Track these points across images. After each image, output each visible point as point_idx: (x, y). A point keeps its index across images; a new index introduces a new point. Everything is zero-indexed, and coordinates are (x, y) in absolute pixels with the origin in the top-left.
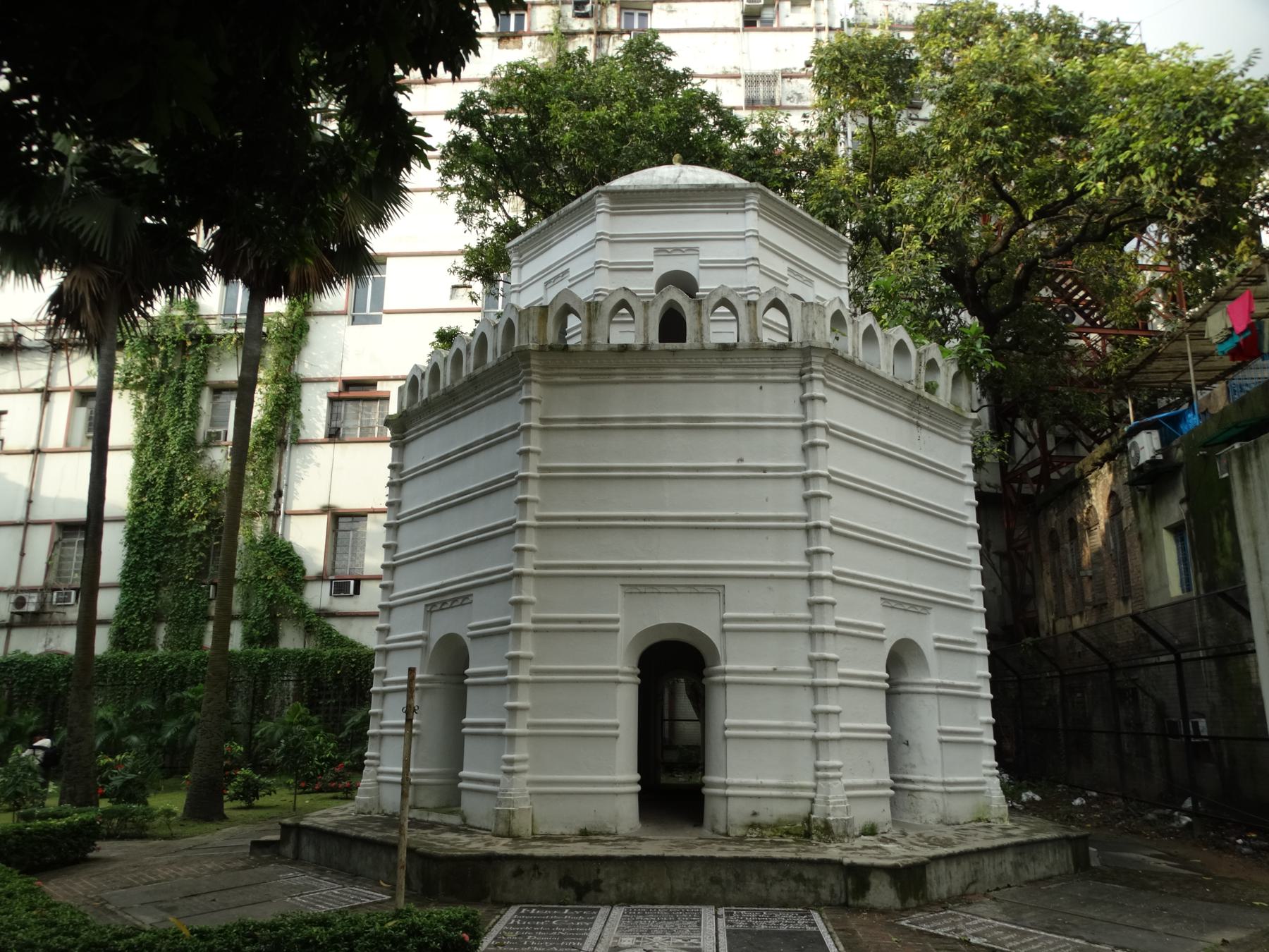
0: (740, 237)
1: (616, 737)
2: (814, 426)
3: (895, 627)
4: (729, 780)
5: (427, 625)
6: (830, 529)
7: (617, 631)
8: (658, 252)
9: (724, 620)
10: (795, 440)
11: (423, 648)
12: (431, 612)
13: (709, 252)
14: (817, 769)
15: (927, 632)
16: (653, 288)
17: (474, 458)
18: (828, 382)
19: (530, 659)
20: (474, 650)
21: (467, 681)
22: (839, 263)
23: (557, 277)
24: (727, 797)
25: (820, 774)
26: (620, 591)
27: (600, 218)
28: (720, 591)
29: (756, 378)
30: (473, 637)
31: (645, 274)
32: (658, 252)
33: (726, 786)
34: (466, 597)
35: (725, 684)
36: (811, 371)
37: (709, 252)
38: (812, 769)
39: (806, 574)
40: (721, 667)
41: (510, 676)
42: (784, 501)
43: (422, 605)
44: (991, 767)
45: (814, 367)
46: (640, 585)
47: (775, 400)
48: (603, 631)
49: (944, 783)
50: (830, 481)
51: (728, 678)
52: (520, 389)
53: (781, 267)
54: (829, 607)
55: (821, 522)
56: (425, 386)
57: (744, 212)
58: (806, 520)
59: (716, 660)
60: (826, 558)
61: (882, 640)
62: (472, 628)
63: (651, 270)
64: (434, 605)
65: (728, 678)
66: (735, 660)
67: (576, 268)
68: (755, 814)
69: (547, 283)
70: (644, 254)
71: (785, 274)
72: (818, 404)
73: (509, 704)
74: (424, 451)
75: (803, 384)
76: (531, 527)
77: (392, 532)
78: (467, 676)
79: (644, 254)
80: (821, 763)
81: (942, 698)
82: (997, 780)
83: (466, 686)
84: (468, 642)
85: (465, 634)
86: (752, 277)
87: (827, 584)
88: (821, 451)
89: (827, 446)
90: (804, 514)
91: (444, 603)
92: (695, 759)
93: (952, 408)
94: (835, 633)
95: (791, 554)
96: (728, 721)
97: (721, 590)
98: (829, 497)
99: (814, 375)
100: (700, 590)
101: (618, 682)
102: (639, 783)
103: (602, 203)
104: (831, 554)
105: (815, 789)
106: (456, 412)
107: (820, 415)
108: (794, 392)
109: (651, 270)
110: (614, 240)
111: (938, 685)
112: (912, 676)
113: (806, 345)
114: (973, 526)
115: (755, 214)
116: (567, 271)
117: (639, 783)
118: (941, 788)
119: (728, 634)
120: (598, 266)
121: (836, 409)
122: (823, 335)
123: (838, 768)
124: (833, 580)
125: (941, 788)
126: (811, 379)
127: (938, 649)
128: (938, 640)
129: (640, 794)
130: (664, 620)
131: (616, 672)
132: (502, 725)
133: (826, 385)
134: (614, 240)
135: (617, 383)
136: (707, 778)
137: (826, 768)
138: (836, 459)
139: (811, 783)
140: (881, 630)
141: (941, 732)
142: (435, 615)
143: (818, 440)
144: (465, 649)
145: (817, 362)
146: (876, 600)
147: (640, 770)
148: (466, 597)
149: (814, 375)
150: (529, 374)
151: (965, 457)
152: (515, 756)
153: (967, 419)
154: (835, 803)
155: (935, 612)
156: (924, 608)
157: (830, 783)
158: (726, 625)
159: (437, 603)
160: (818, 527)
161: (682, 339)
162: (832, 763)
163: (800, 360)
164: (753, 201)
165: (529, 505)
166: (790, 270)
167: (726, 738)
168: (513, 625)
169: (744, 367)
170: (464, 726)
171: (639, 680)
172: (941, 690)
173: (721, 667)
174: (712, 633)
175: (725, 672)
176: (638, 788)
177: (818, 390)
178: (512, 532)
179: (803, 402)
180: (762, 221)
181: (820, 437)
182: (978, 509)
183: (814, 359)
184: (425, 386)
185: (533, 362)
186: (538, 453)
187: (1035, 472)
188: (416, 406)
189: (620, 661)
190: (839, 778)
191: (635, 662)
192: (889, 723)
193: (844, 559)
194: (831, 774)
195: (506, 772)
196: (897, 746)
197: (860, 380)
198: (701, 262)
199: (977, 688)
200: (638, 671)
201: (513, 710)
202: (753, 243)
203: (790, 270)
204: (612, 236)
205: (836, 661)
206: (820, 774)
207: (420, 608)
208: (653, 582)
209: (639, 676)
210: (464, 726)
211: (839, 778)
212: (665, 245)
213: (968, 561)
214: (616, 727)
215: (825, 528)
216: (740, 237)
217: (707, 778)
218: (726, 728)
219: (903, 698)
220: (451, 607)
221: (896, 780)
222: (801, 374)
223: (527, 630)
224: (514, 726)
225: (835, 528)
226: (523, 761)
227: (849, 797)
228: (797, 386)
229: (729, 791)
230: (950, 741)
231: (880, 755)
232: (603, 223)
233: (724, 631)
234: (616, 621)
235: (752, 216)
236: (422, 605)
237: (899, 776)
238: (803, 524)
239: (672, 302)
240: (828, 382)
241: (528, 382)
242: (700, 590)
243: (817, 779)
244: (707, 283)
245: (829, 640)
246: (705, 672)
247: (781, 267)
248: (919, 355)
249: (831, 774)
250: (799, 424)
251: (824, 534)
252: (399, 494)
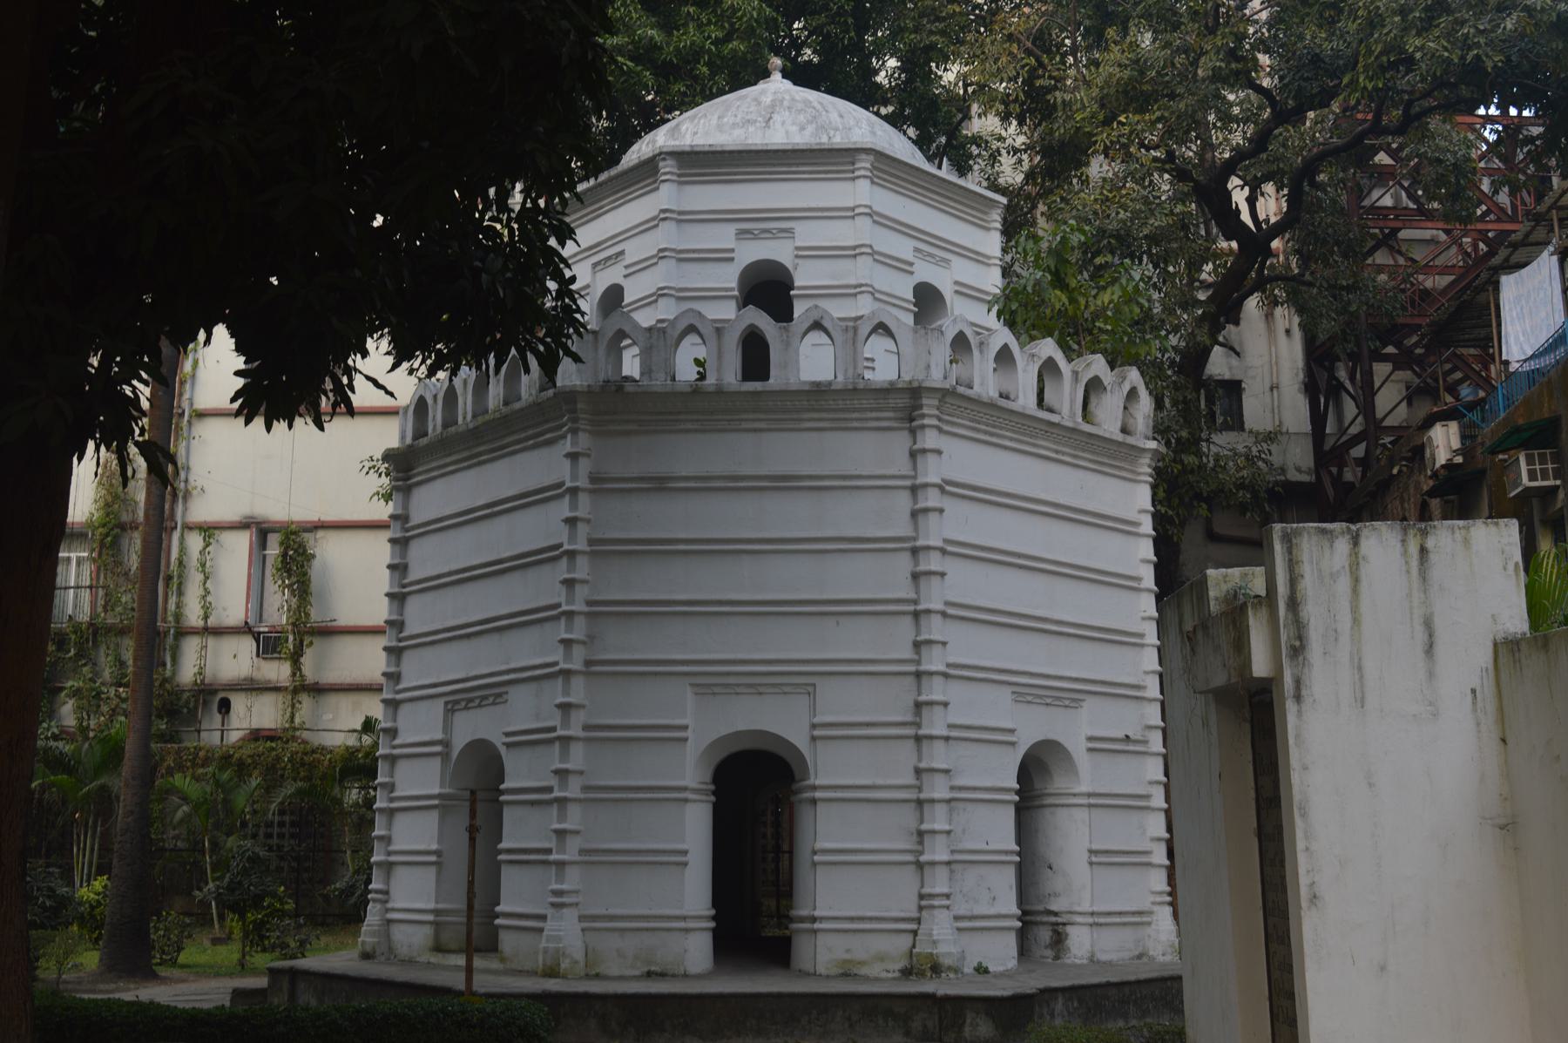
0: (850, 213)
1: (686, 864)
2: (926, 486)
3: (1033, 726)
4: (817, 913)
5: (447, 726)
6: (944, 614)
7: (686, 740)
8: (742, 234)
9: (814, 726)
10: (903, 502)
11: (445, 756)
12: (453, 711)
13: (810, 234)
14: (921, 897)
15: (1073, 729)
16: (734, 284)
17: (504, 519)
18: (946, 428)
19: (581, 773)
20: (510, 760)
21: (502, 798)
22: (988, 229)
23: (609, 258)
24: (815, 931)
25: (924, 903)
26: (689, 691)
27: (664, 188)
28: (810, 691)
29: (855, 424)
30: (508, 745)
31: (724, 265)
32: (742, 234)
33: (814, 919)
34: (499, 695)
35: (814, 801)
36: (923, 416)
37: (810, 234)
38: (915, 898)
39: (912, 668)
40: (811, 781)
41: (557, 794)
42: (887, 578)
43: (441, 702)
44: (1161, 893)
45: (925, 411)
46: (713, 682)
47: (873, 451)
48: (671, 736)
49: (1092, 914)
50: (944, 552)
51: (818, 794)
52: (563, 437)
53: (902, 247)
54: (941, 708)
55: (932, 606)
56: (436, 416)
57: (853, 179)
58: (916, 602)
59: (806, 775)
60: (937, 649)
61: (1013, 744)
62: (507, 734)
63: (732, 259)
64: (457, 702)
65: (818, 794)
66: (828, 769)
67: (636, 250)
68: (848, 951)
69: (595, 265)
70: (723, 236)
71: (909, 256)
72: (931, 458)
73: (557, 826)
74: (432, 500)
75: (913, 432)
76: (580, 613)
77: (396, 603)
78: (502, 792)
79: (723, 236)
80: (926, 890)
81: (1093, 810)
82: (1168, 910)
83: (502, 804)
84: (503, 750)
85: (498, 740)
86: (862, 271)
87: (937, 680)
88: (933, 517)
89: (941, 511)
90: (912, 595)
91: (471, 700)
92: (784, 889)
93: (1120, 437)
94: (947, 739)
95: (895, 641)
96: (818, 846)
97: (811, 689)
98: (943, 575)
99: (926, 421)
100: (786, 689)
101: (686, 800)
102: (714, 918)
103: (667, 167)
104: (944, 644)
105: (919, 921)
106: (480, 454)
107: (932, 472)
108: (899, 443)
109: (732, 259)
110: (683, 218)
111: (1089, 795)
112: (1059, 783)
113: (915, 384)
114: (1149, 590)
115: (868, 182)
116: (622, 253)
117: (714, 918)
118: (1090, 920)
119: (819, 744)
120: (662, 254)
121: (958, 457)
122: (937, 369)
123: (948, 896)
124: (946, 675)
125: (1090, 920)
126: (923, 427)
127: (1090, 750)
128: (1090, 739)
129: (714, 930)
130: (742, 725)
131: (685, 789)
132: (549, 851)
133: (940, 430)
134: (683, 218)
135: (688, 431)
136: (794, 913)
137: (932, 896)
138: (958, 522)
139: (915, 914)
140: (1012, 731)
141: (1091, 852)
142: (457, 714)
143: (930, 504)
144: (499, 757)
145: (929, 406)
146: (1005, 694)
147: (717, 900)
148: (499, 695)
149: (926, 421)
150: (575, 420)
151: (1142, 496)
152: (564, 887)
153: (1144, 450)
154: (942, 937)
155: (1090, 703)
156: (1074, 700)
157: (936, 912)
158: (816, 733)
159: (462, 698)
160: (928, 611)
161: (765, 376)
162: (938, 890)
163: (906, 405)
164: (864, 163)
165: (578, 587)
166: (917, 250)
167: (814, 864)
168: (560, 732)
169: (843, 410)
170: (501, 852)
171: (713, 798)
172: (1092, 801)
173: (811, 781)
174: (800, 739)
175: (814, 788)
176: (712, 924)
177: (930, 439)
178: (556, 618)
179: (913, 455)
180: (877, 190)
181: (932, 499)
182: (1157, 567)
183: (925, 401)
184: (436, 416)
185: (580, 406)
186: (588, 521)
187: (1359, 451)
188: (424, 441)
189: (689, 770)
190: (948, 907)
191: (708, 777)
192: (1019, 842)
193: (965, 645)
194: (936, 902)
195: (553, 905)
196: (1029, 867)
197: (994, 420)
198: (797, 248)
199: (1147, 797)
200: (712, 787)
201: (561, 834)
202: (863, 223)
203: (917, 250)
204: (680, 213)
205: (947, 771)
206: (924, 903)
207: (439, 705)
208: (732, 680)
209: (714, 793)
210: (501, 852)
211: (948, 907)
212: (750, 223)
213: (1142, 636)
214: (685, 853)
215: (937, 612)
216: (850, 213)
217: (794, 913)
218: (815, 853)
219: (1047, 811)
220: (480, 706)
221: (1025, 913)
222: (912, 420)
223: (577, 739)
224: (564, 853)
225: (951, 611)
226: (577, 892)
227: (959, 929)
228: (906, 433)
229: (816, 926)
230: (1100, 858)
231: (1008, 877)
232: (666, 196)
233: (814, 739)
234: (685, 728)
235: (864, 186)
236: (441, 701)
237: (1028, 908)
238: (911, 608)
239: (752, 326)
240: (946, 428)
241: (574, 431)
242: (786, 689)
243: (921, 908)
244: (805, 276)
245: (939, 746)
246: (795, 786)
247: (902, 247)
248: (1075, 373)
249: (936, 902)
250: (908, 483)
251: (936, 620)
252: (403, 554)
